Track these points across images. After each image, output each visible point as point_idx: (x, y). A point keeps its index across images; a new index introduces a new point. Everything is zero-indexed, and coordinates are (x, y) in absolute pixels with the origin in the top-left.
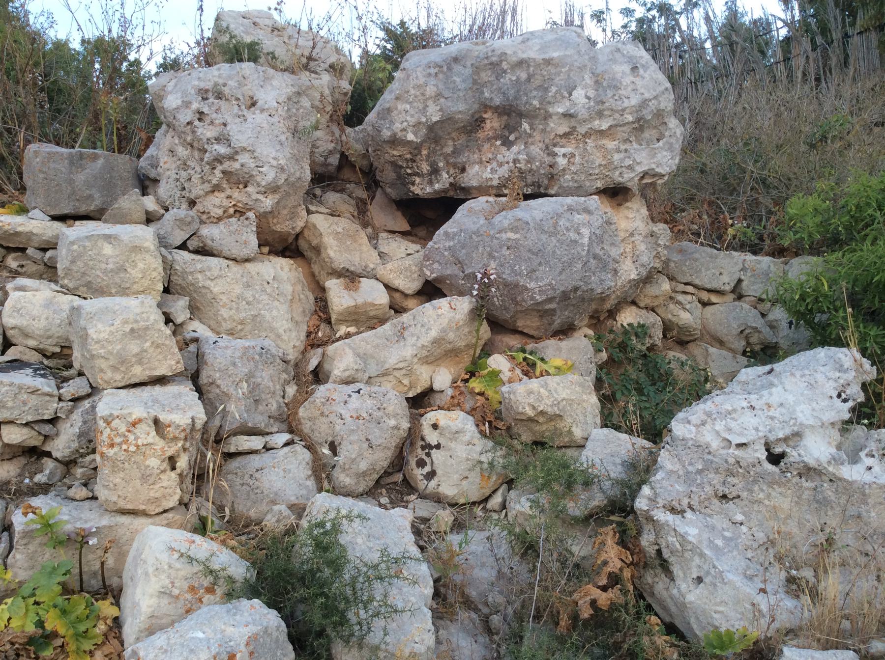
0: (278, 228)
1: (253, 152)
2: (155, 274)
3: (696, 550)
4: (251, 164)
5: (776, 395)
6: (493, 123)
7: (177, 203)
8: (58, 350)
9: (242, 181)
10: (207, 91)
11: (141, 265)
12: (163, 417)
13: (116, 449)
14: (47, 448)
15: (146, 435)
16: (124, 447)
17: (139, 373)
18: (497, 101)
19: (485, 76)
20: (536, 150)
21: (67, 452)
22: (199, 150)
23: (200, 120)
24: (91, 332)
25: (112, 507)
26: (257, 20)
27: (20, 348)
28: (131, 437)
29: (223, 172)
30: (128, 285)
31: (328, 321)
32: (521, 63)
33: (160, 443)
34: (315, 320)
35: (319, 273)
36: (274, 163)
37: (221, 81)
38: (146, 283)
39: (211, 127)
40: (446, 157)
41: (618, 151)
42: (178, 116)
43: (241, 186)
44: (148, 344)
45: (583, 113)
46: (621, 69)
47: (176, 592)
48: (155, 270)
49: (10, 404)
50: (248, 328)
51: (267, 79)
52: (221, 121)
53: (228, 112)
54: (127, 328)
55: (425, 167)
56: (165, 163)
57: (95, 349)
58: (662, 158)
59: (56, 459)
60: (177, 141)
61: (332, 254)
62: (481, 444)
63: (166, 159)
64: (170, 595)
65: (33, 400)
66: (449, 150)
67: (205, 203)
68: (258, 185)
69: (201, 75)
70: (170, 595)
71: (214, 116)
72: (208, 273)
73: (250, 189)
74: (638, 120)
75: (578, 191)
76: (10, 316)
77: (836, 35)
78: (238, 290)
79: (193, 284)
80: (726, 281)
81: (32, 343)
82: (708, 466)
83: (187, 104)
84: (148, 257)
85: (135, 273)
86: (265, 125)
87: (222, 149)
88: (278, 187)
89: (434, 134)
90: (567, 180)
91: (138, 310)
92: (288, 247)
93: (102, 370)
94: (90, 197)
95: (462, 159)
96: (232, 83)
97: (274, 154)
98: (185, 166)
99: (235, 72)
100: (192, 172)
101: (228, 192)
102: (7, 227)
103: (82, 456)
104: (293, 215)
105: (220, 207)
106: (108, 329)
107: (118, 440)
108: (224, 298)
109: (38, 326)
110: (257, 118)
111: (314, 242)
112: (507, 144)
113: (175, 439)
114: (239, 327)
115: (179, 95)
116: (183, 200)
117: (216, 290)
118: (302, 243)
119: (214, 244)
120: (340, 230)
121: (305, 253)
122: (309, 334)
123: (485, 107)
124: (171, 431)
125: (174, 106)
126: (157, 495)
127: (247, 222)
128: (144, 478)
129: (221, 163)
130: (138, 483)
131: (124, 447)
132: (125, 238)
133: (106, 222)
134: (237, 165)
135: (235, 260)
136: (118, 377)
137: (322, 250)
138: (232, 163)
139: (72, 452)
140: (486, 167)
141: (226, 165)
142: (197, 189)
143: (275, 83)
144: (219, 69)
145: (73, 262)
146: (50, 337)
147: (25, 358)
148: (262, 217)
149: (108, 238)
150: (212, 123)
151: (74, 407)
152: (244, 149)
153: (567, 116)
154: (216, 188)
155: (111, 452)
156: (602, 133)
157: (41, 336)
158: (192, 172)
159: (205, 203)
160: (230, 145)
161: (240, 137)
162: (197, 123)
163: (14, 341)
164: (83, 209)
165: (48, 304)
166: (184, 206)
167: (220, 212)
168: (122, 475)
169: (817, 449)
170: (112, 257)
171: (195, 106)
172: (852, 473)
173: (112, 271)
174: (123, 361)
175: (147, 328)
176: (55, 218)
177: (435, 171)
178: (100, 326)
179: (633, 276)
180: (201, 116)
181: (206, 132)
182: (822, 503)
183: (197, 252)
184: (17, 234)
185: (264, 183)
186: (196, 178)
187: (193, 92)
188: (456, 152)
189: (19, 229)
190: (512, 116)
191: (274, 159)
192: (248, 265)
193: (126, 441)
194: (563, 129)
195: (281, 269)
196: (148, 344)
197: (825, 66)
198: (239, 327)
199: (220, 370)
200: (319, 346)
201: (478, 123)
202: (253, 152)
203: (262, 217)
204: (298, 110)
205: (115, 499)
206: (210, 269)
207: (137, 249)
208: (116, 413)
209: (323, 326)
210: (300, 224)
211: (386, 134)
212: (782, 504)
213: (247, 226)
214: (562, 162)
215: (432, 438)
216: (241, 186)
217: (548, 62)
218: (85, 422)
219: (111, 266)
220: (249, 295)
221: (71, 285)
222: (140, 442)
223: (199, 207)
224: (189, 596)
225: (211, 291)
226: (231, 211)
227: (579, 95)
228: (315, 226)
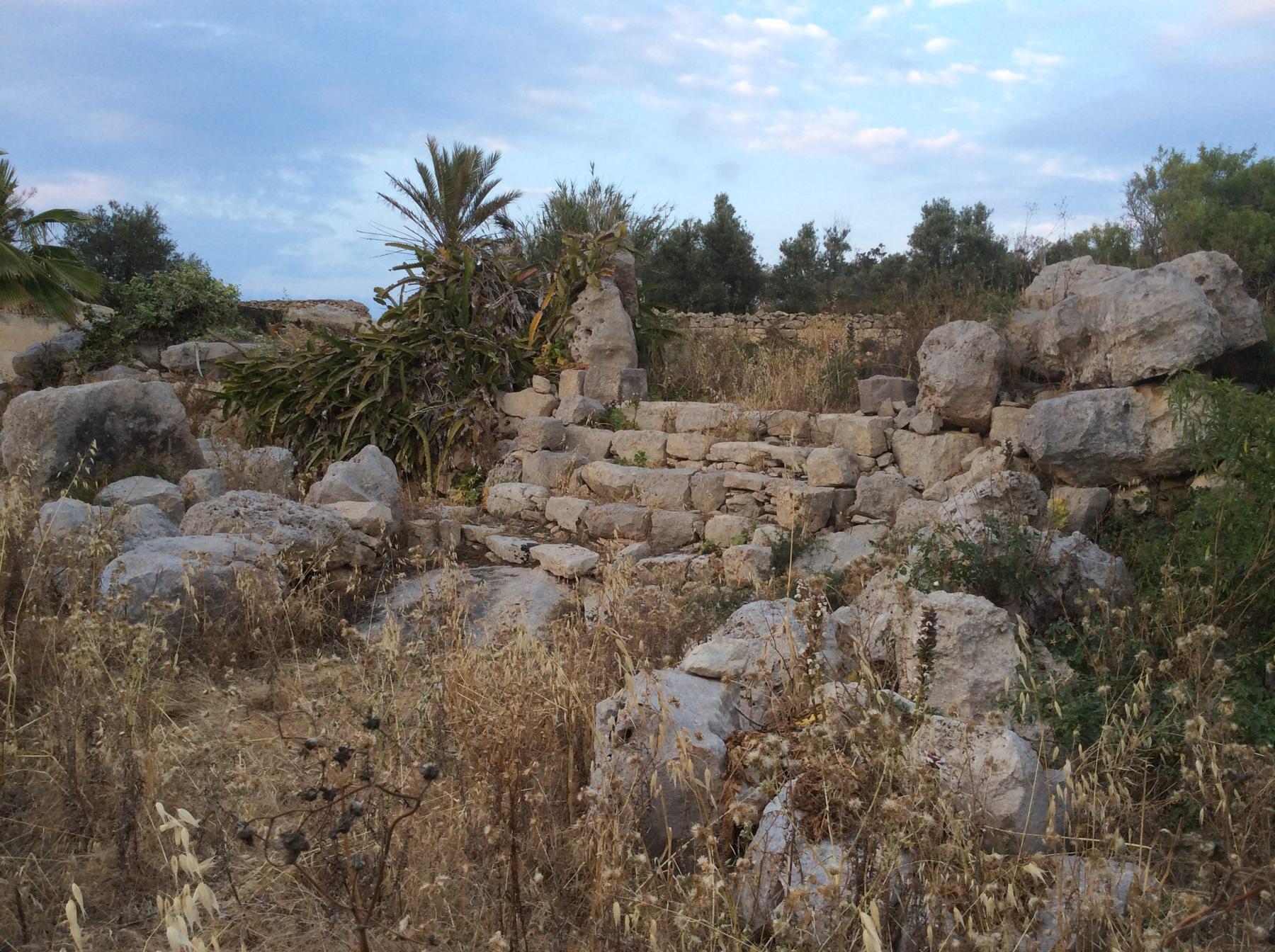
0: (964, 416)
15: (787, 497)
40: (1074, 364)
41: (1134, 354)
66: (1076, 359)
74: (1142, 332)
104: (976, 408)
179: (1171, 446)
188: (1079, 361)
207: (860, 428)
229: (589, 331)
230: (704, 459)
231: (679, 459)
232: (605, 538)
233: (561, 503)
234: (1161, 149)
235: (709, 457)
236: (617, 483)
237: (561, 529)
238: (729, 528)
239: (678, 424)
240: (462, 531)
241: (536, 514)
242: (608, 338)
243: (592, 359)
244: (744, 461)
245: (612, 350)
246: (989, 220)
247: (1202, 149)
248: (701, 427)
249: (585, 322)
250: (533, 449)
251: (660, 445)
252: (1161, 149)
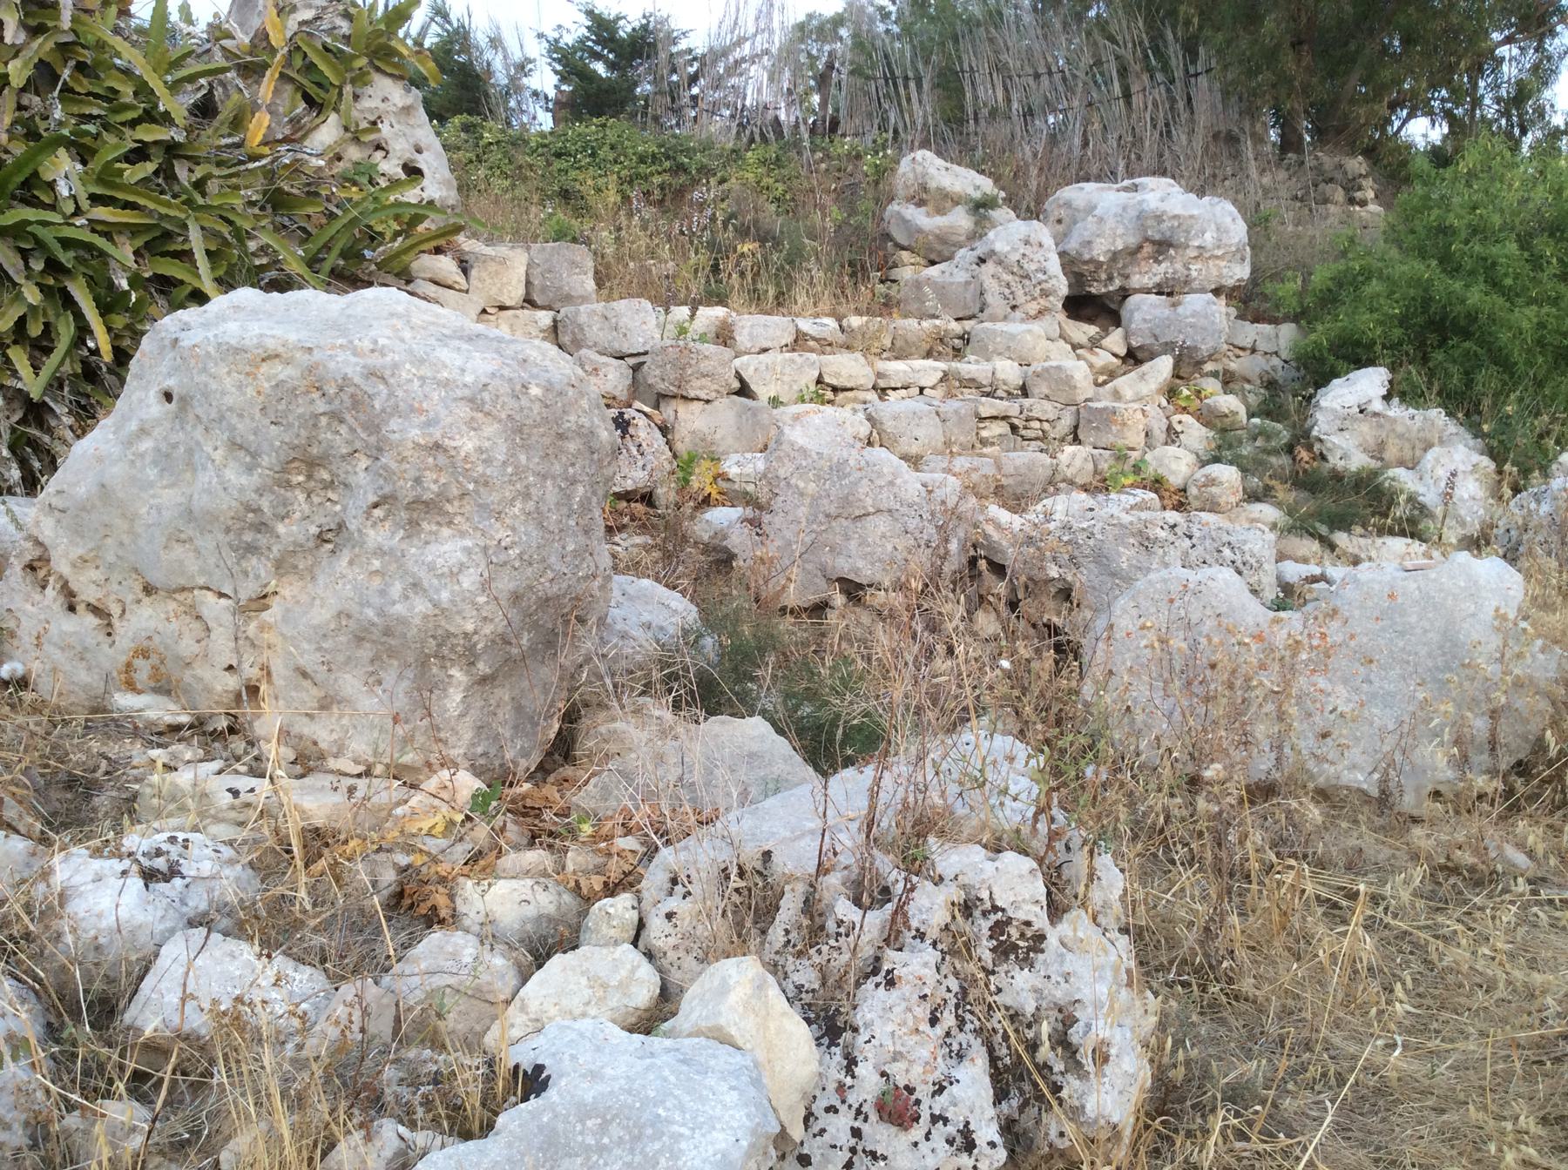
3: (1340, 447)
5: (1358, 387)
6: (1148, 249)
9: (1045, 294)
18: (1157, 237)
19: (1150, 222)
20: (1179, 266)
32: (1176, 217)
45: (1209, 246)
46: (1228, 220)
55: (1104, 276)
58: (1240, 272)
62: (1204, 429)
75: (1202, 291)
77: (1178, 74)
80: (1247, 343)
82: (1337, 417)
83: (1015, 250)
87: (1040, 276)
89: (1114, 256)
90: (1195, 285)
95: (1127, 271)
98: (1008, 286)
112: (1159, 263)
123: (1147, 240)
140: (1145, 275)
141: (1044, 286)
153: (1199, 247)
154: (1034, 299)
156: (1217, 257)
169: (1378, 405)
172: (1391, 413)
176: (957, 319)
177: (1110, 279)
182: (1380, 426)
188: (1124, 267)
190: (1163, 247)
194: (1195, 254)
197: (1172, 108)
201: (1140, 247)
211: (1087, 257)
212: (1365, 429)
214: (1194, 274)
215: (1179, 428)
217: (1191, 217)
227: (1208, 236)
235: (882, 383)
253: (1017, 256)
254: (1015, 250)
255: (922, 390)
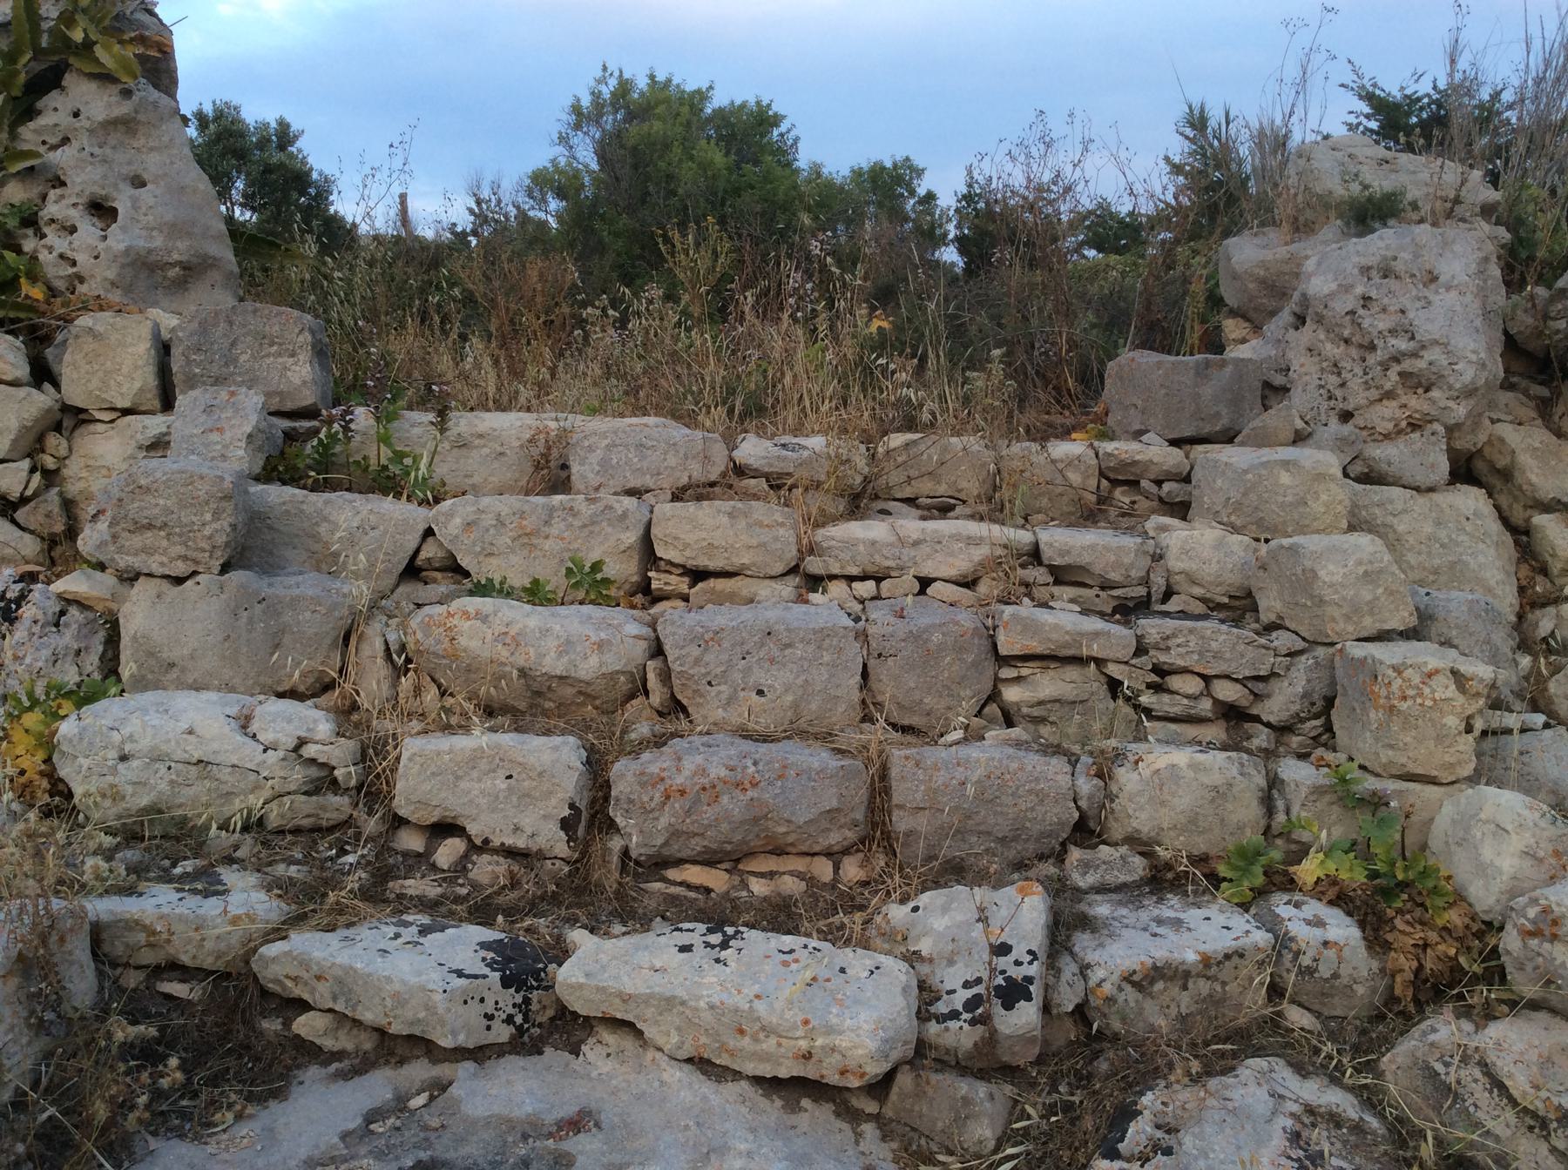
1: (1446, 345)
2: (1340, 508)
4: (1444, 361)
7: (1323, 417)
8: (1226, 600)
9: (1419, 383)
10: (1369, 268)
11: (1324, 497)
12: (1462, 669)
13: (1410, 702)
14: (1255, 711)
15: (1445, 689)
16: (1419, 701)
17: (1370, 625)
21: (1284, 716)
22: (1361, 346)
23: (1364, 306)
24: (1322, 573)
25: (1394, 772)
26: (1350, 150)
27: (1183, 597)
28: (1427, 691)
29: (1400, 374)
30: (1307, 522)
31: (1544, 571)
33: (1461, 699)
34: (1525, 571)
35: (1510, 506)
36: (1474, 358)
37: (1389, 254)
38: (1328, 519)
39: (1382, 316)
42: (1331, 304)
43: (1420, 391)
44: (1380, 590)
47: (1541, 854)
48: (1340, 502)
49: (1228, 655)
50: (1443, 578)
51: (1445, 244)
52: (1397, 308)
53: (1404, 295)
54: (1361, 570)
56: (1302, 365)
57: (1329, 596)
59: (1268, 725)
60: (1322, 337)
61: (1534, 479)
63: (1302, 360)
64: (1534, 857)
65: (1251, 653)
67: (1367, 416)
68: (1450, 388)
69: (1360, 248)
70: (1534, 857)
71: (1386, 301)
72: (1390, 507)
73: (1435, 393)
76: (1177, 559)
78: (1428, 528)
79: (1367, 522)
81: (1198, 591)
83: (1346, 288)
84: (1332, 486)
85: (1317, 507)
86: (1458, 308)
87: (1403, 344)
88: (1476, 389)
91: (1371, 549)
92: (1464, 471)
93: (1333, 620)
94: (1217, 415)
96: (1405, 255)
97: (1472, 346)
98: (1336, 368)
99: (1408, 240)
100: (1349, 376)
101: (1404, 399)
102: (1124, 456)
103: (1302, 721)
105: (1390, 420)
106: (1342, 571)
107: (1411, 692)
108: (1411, 539)
109: (1209, 571)
110: (1444, 300)
111: (1501, 462)
113: (1478, 694)
114: (1431, 578)
115: (1330, 276)
116: (1332, 413)
117: (1401, 528)
118: (1479, 466)
119: (1392, 469)
120: (1537, 445)
121: (1484, 479)
122: (1522, 590)
124: (1474, 686)
125: (1326, 291)
126: (1452, 760)
127: (1433, 438)
128: (1439, 739)
129: (1398, 361)
130: (1432, 743)
131: (1419, 701)
132: (1307, 464)
133: (1242, 444)
134: (1421, 364)
135: (1417, 489)
136: (1350, 629)
137: (1516, 474)
138: (1413, 361)
139: (1292, 717)
141: (1407, 365)
142: (1357, 396)
143: (1457, 248)
144: (1381, 238)
145: (1245, 494)
146: (1220, 584)
147: (1188, 609)
148: (1450, 430)
149: (1286, 464)
150: (1384, 310)
151: (1292, 664)
152: (1436, 342)
154: (1389, 395)
155: (1404, 706)
157: (1211, 583)
158: (1349, 376)
159: (1367, 416)
160: (1413, 338)
161: (1429, 327)
162: (1361, 312)
163: (1176, 588)
164: (1207, 429)
165: (1219, 545)
166: (1334, 423)
167: (1390, 426)
168: (1413, 733)
170: (1289, 487)
171: (1359, 290)
173: (1291, 504)
174: (1355, 611)
175: (1380, 571)
176: (1174, 443)
178: (1331, 567)
180: (1366, 300)
181: (1375, 323)
183: (1358, 480)
184: (1135, 463)
185: (1458, 386)
186: (1355, 384)
187: (1356, 271)
189: (1138, 457)
191: (1474, 352)
192: (1434, 496)
193: (1421, 695)
195: (1470, 500)
196: (1380, 590)
198: (1431, 578)
199: (1457, 627)
200: (1544, 605)
202: (1446, 345)
203: (1450, 430)
204: (1485, 281)
205: (1404, 760)
206: (1391, 502)
207: (1320, 477)
208: (1409, 662)
209: (1539, 578)
210: (1482, 438)
213: (1434, 444)
216: (1420, 391)
218: (1309, 681)
219: (1289, 499)
220: (1442, 534)
221: (1238, 523)
222: (1437, 696)
223: (1358, 420)
224: (1553, 861)
225: (1395, 531)
226: (1404, 424)
228: (1502, 440)
229: (102, 210)
230: (794, 570)
231: (698, 575)
232: (709, 860)
233: (475, 757)
234: (605, 68)
235: (814, 565)
236: (589, 667)
237: (484, 847)
238: (1219, 794)
239: (580, 471)
240: (97, 934)
241: (337, 805)
242: (175, 229)
243: (128, 290)
244: (951, 572)
245: (186, 267)
246: (299, 144)
247: (652, 77)
248: (667, 483)
249: (84, 179)
250: (180, 569)
251: (631, 537)
252: (605, 68)
253: (1349, 302)
254: (1346, 288)
255: (925, 583)
